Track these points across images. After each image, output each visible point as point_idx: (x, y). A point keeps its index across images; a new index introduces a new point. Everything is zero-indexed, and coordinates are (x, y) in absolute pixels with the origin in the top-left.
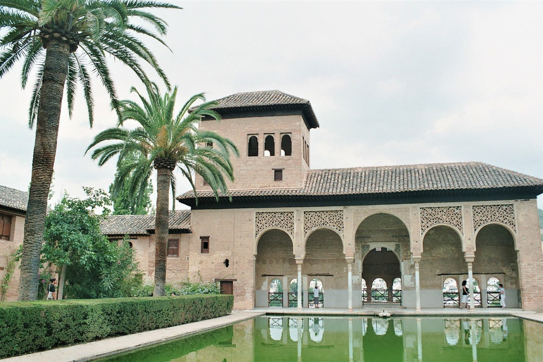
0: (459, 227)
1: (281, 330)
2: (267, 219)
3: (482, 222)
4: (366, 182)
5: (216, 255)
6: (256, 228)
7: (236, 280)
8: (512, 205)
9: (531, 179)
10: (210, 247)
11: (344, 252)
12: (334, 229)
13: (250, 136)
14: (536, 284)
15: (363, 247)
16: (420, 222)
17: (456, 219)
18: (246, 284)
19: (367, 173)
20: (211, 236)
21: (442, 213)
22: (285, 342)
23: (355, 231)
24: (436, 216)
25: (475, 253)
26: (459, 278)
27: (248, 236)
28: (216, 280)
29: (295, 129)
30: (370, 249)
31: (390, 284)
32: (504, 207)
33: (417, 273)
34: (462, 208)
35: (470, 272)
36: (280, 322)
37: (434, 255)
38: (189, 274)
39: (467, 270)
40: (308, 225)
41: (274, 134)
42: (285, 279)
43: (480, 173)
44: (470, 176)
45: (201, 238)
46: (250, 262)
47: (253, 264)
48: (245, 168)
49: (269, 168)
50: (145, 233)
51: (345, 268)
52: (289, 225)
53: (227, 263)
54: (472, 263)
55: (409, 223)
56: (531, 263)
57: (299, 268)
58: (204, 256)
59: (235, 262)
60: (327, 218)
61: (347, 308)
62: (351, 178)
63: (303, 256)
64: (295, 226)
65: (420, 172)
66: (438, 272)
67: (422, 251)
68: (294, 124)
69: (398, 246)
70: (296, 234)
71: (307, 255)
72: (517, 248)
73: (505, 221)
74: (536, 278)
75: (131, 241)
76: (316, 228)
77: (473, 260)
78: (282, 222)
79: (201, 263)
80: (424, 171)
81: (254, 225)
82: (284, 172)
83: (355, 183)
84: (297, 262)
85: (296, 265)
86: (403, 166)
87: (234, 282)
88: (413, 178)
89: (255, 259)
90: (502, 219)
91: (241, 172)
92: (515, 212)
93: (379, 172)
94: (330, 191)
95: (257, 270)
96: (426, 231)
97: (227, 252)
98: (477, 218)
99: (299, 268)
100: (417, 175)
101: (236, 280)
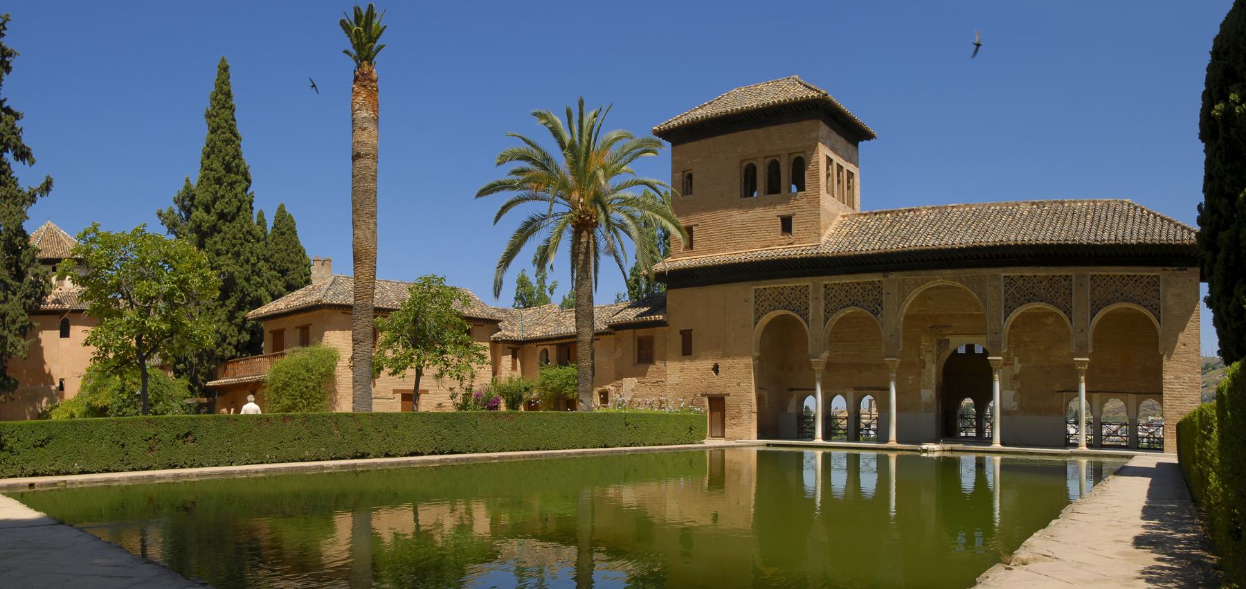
13: (745, 164)
15: (939, 343)
30: (952, 347)
35: (1083, 386)
43: (1116, 219)
56: (1181, 374)
80: (1026, 213)
81: (752, 309)
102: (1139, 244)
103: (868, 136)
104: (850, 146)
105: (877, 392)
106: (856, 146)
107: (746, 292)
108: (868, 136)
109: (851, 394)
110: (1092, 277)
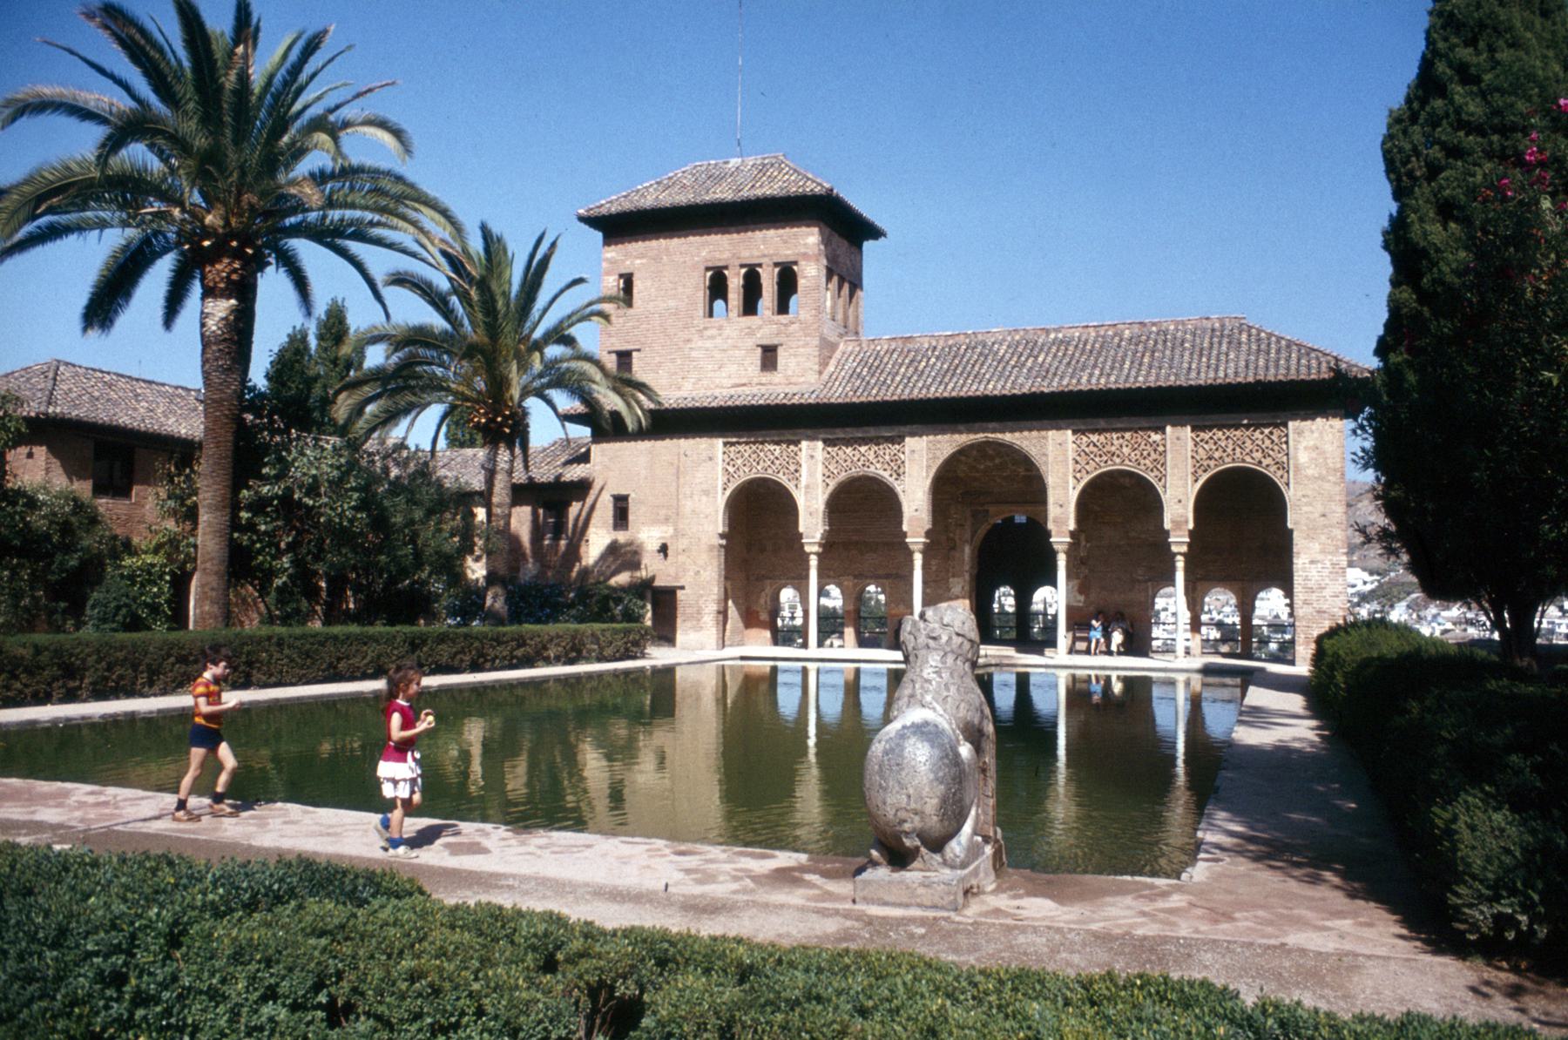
0: (1156, 473)
3: (1212, 463)
7: (682, 588)
10: (631, 517)
11: (905, 528)
14: (1325, 607)
16: (1071, 462)
17: (1153, 456)
20: (633, 495)
23: (928, 482)
24: (1108, 448)
25: (1191, 534)
27: (706, 493)
29: (805, 256)
37: (1133, 534)
39: (1173, 570)
41: (760, 265)
46: (711, 548)
48: (700, 344)
49: (750, 343)
51: (933, 562)
52: (792, 468)
53: (664, 549)
55: (1046, 463)
56: (1319, 557)
63: (818, 537)
64: (804, 471)
67: (1072, 526)
70: (807, 487)
72: (1290, 525)
73: (1265, 462)
74: (1327, 593)
77: (1184, 549)
82: (780, 351)
84: (807, 549)
87: (680, 593)
89: (724, 542)
90: (1258, 455)
91: (694, 354)
96: (1082, 484)
97: (664, 528)
98: (1202, 454)
101: (682, 588)
102: (1258, 382)
103: (875, 233)
104: (854, 249)
106: (860, 247)
107: (715, 446)
108: (875, 233)
109: (849, 582)
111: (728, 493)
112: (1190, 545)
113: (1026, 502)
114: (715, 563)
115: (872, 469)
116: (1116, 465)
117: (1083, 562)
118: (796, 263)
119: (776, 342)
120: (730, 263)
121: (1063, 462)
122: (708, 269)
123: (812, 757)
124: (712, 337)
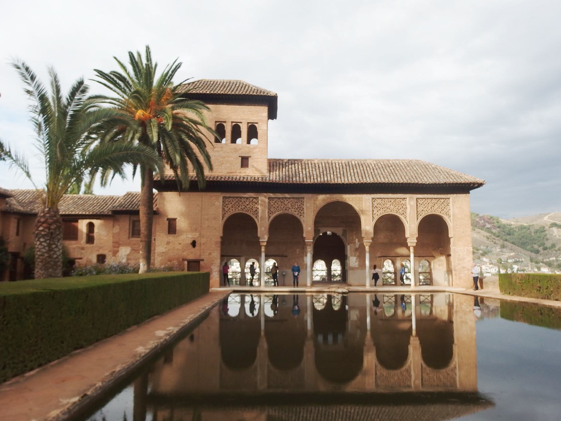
1: (239, 305)
2: (233, 203)
4: (325, 173)
5: (183, 237)
6: (223, 211)
8: (449, 198)
9: (466, 177)
11: (304, 235)
12: (296, 214)
13: (218, 123)
16: (371, 210)
18: (212, 264)
19: (324, 165)
21: (388, 204)
22: (242, 317)
26: (396, 260)
27: (215, 218)
28: (184, 260)
31: (329, 265)
32: (442, 200)
33: (367, 255)
34: (408, 200)
36: (238, 299)
38: (156, 255)
40: (272, 210)
42: (243, 259)
44: (415, 172)
45: (168, 219)
46: (216, 243)
47: (219, 245)
50: (110, 213)
51: (298, 250)
53: (194, 244)
54: (414, 247)
57: (263, 249)
58: (171, 238)
59: (202, 244)
60: (289, 204)
61: (305, 286)
62: (310, 169)
65: (371, 167)
66: (379, 254)
68: (258, 114)
69: (345, 232)
70: (261, 217)
71: (269, 238)
75: (94, 221)
76: (279, 212)
77: (415, 245)
78: (248, 207)
79: (168, 243)
82: (250, 159)
83: (314, 173)
84: (261, 244)
85: (260, 247)
86: (355, 160)
87: (201, 263)
88: (366, 171)
90: (440, 210)
92: (451, 205)
93: (334, 165)
94: (294, 179)
95: (222, 250)
97: (195, 233)
99: (263, 249)
100: (368, 169)
101: (203, 260)
105: (278, 258)
110: (417, 199)
111: (225, 219)
112: (417, 243)
113: (334, 227)
114: (219, 249)
115: (290, 210)
116: (389, 212)
117: (357, 250)
118: (257, 123)
119: (247, 155)
120: (226, 120)
121: (368, 210)
122: (216, 122)
123: (262, 333)
124: (218, 151)
